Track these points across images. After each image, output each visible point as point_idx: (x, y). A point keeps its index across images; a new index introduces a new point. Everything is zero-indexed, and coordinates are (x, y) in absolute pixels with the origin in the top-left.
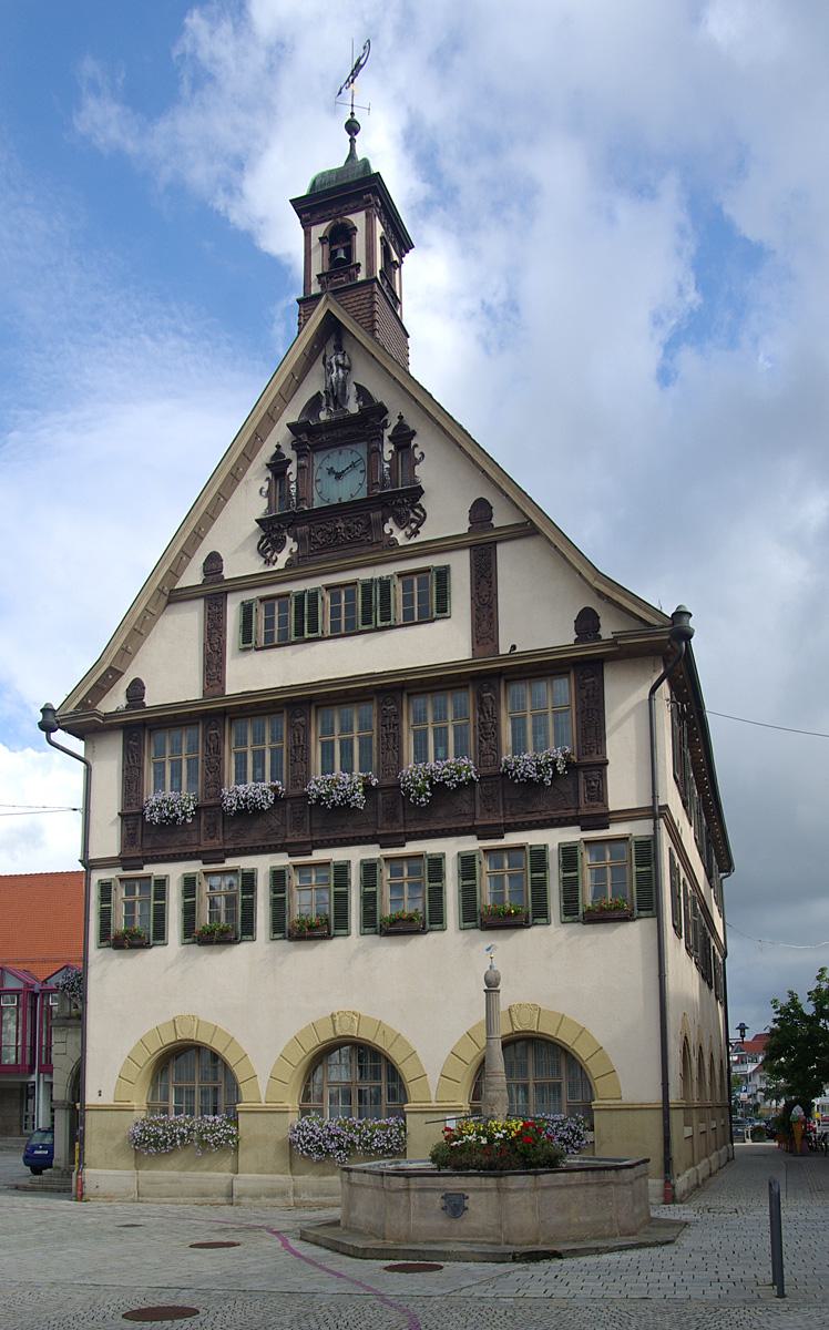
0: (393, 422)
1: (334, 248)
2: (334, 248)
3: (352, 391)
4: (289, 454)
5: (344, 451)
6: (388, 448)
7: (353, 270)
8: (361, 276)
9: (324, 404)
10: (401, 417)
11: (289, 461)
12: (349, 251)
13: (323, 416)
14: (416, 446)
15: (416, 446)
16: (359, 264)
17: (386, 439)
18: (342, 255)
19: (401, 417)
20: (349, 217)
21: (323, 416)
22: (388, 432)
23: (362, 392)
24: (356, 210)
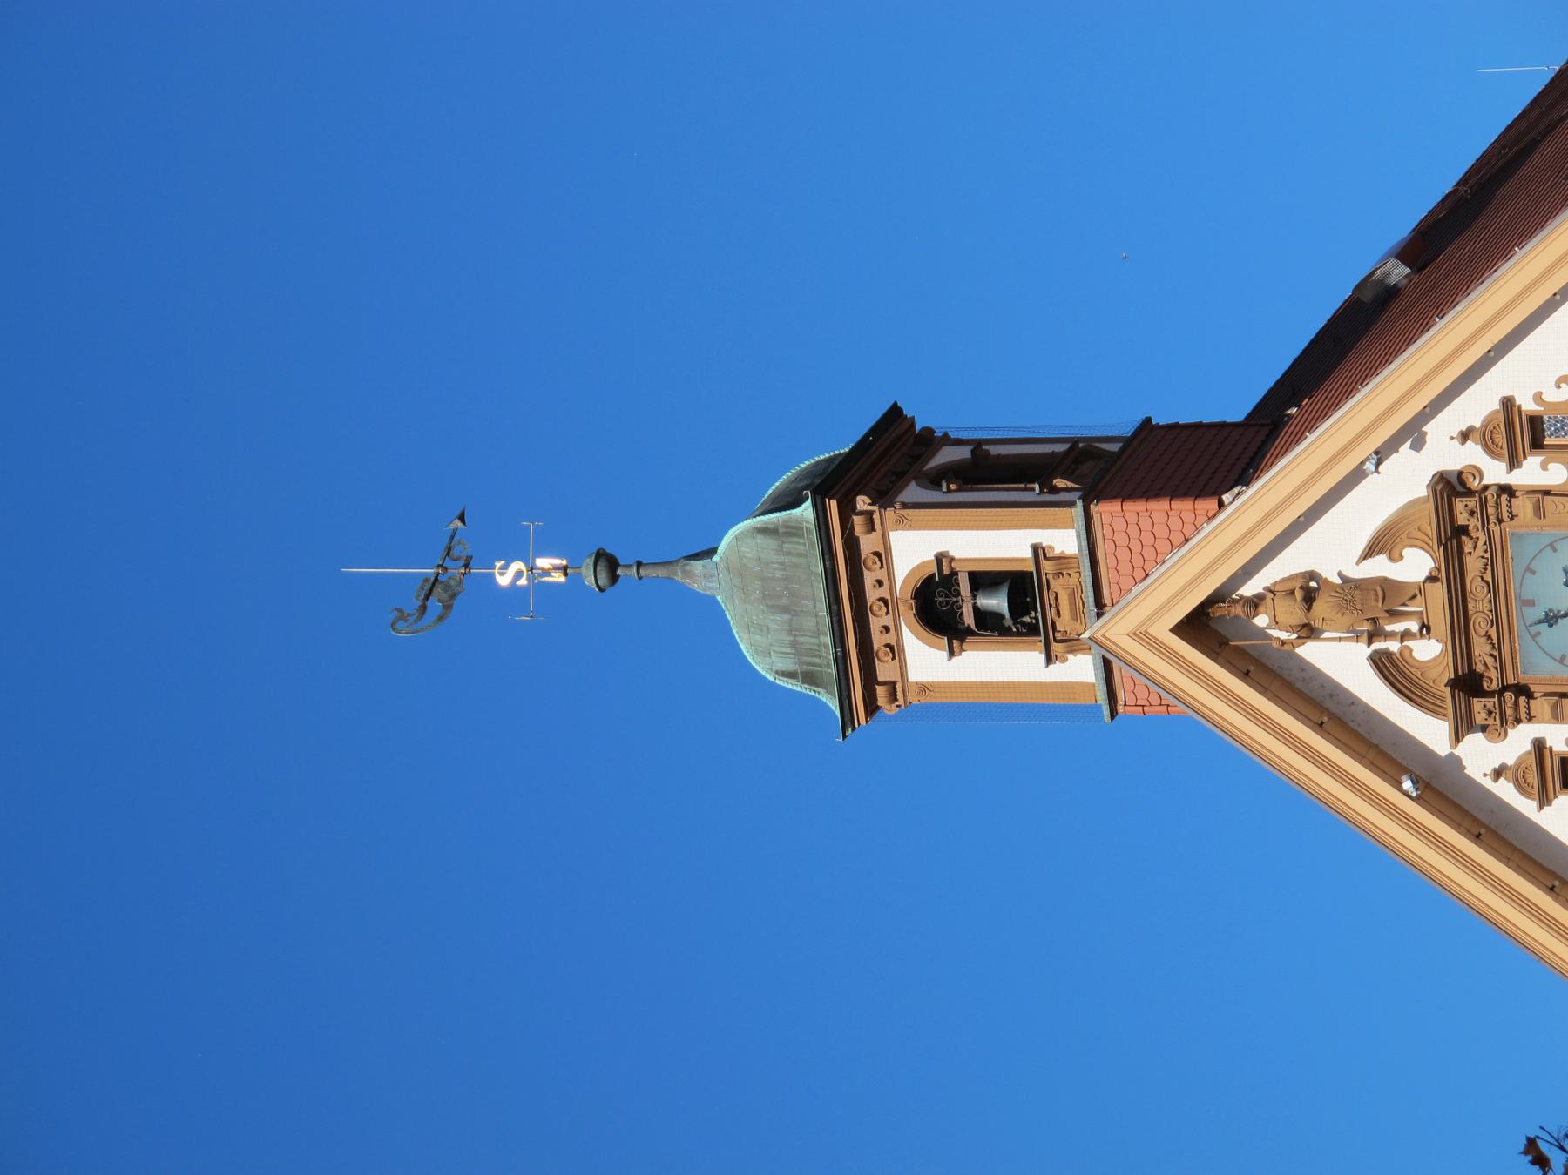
0: (1473, 455)
1: (969, 620)
2: (969, 620)
3: (1379, 567)
4: (1519, 740)
5: (1527, 596)
6: (1533, 472)
7: (1047, 567)
8: (1065, 540)
9: (1394, 646)
10: (1465, 436)
11: (1539, 746)
12: (983, 580)
13: (1427, 651)
14: (1538, 397)
15: (1538, 397)
16: (1036, 549)
17: (1518, 478)
18: (997, 602)
19: (1465, 436)
20: (900, 575)
21: (1427, 651)
22: (1495, 472)
23: (1383, 543)
24: (883, 557)
